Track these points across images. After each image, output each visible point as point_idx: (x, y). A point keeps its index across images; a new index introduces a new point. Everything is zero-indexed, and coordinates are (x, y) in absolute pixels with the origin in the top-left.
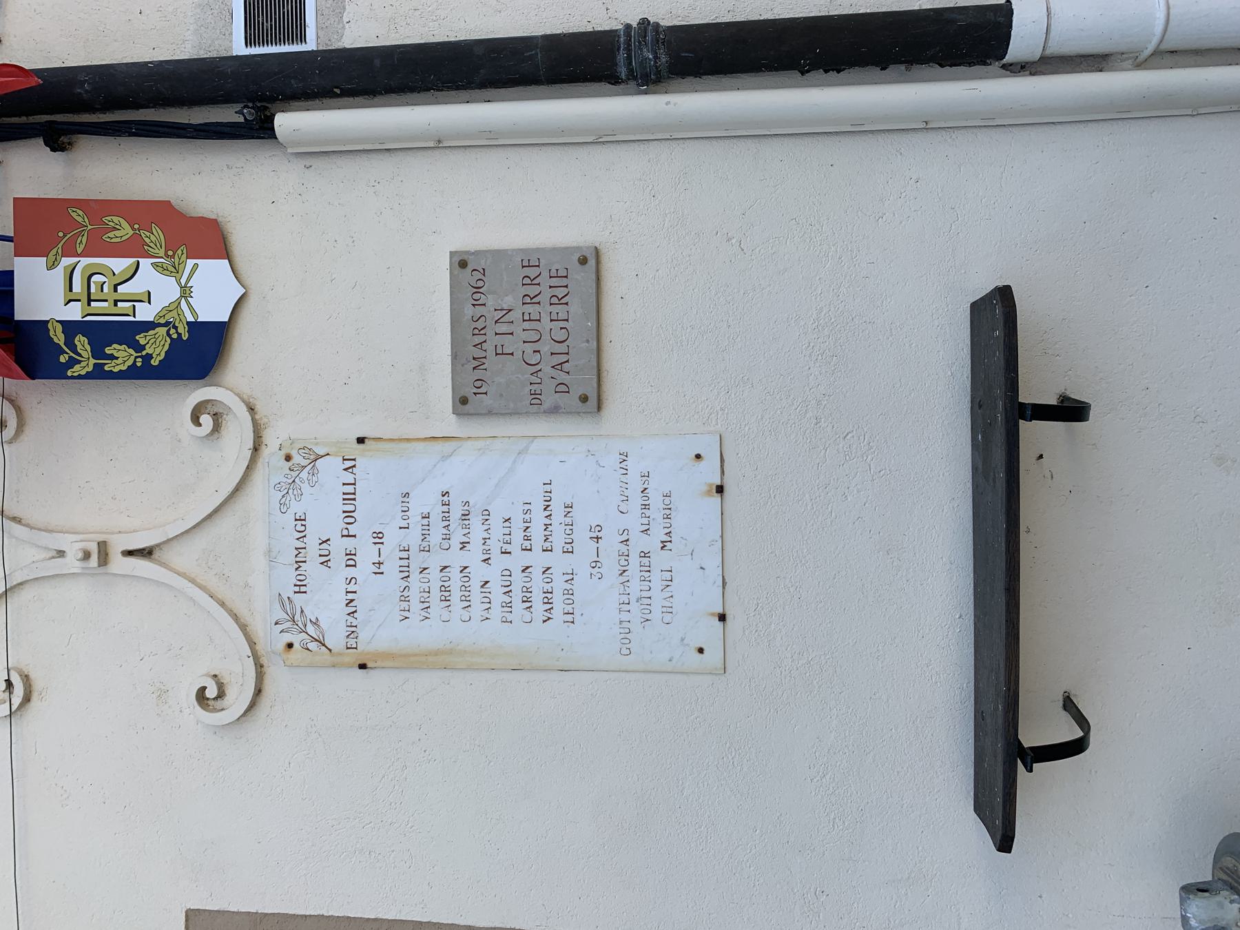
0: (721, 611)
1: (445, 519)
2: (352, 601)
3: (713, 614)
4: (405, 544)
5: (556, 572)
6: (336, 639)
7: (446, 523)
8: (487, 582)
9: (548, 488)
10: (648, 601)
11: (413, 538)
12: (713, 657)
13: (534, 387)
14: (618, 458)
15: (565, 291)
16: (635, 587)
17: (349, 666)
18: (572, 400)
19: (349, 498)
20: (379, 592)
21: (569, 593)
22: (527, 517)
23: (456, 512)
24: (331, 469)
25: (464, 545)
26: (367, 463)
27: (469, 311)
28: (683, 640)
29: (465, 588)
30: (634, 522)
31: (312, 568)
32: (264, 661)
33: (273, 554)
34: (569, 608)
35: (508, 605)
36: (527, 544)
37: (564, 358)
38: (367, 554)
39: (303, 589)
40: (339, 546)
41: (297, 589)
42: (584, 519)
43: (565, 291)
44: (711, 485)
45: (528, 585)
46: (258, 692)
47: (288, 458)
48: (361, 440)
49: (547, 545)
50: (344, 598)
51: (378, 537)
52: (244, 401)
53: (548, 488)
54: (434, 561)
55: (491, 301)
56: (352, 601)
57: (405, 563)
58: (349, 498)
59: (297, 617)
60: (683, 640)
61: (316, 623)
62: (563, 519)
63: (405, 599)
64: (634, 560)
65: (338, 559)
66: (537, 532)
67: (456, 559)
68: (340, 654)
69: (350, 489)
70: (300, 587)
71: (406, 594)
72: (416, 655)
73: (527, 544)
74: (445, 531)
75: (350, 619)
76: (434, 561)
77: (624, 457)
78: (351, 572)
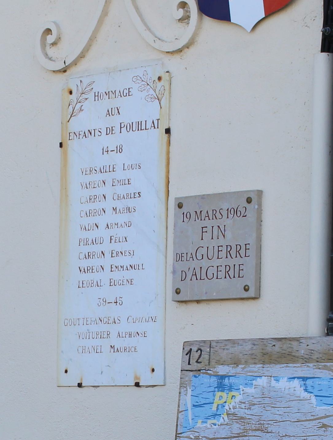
0: (83, 385)
3: (81, 379)
6: (76, 125)
10: (88, 337)
15: (232, 276)
22: (127, 253)
23: (131, 203)
27: (225, 206)
30: (124, 327)
37: (198, 277)
38: (111, 142)
43: (232, 276)
44: (139, 379)
50: (91, 128)
55: (229, 222)
77: (154, 320)
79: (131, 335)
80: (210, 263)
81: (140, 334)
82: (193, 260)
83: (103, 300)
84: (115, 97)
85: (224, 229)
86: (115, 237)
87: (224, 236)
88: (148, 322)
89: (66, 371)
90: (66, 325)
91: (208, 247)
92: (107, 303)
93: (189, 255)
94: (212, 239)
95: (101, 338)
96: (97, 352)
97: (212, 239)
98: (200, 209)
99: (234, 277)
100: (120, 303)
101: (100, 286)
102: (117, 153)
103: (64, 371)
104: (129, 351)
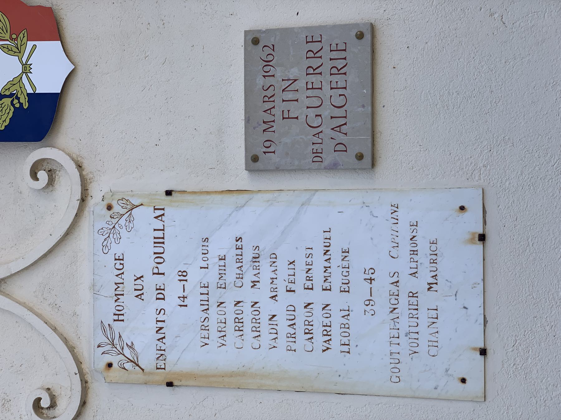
0: (482, 346)
1: (239, 261)
2: (161, 328)
3: (475, 349)
4: (205, 282)
5: (334, 309)
6: (148, 360)
7: (240, 264)
8: (274, 316)
9: (327, 235)
10: (416, 336)
11: (212, 277)
12: (474, 386)
14: (390, 209)
15: (343, 62)
16: (404, 323)
17: (158, 384)
18: (349, 158)
19: (159, 241)
20: (183, 321)
21: (346, 327)
22: (309, 260)
23: (248, 255)
24: (144, 217)
25: (254, 284)
26: (175, 213)
27: (260, 81)
28: (447, 371)
29: (256, 320)
30: (403, 265)
31: (129, 299)
32: (88, 378)
33: (97, 288)
34: (345, 340)
35: (293, 336)
36: (309, 284)
37: (343, 121)
39: (121, 318)
41: (116, 317)
42: (359, 263)
43: (343, 62)
44: (473, 234)
45: (310, 319)
46: (83, 403)
47: (109, 208)
48: (169, 193)
49: (327, 285)
50: (154, 326)
51: (183, 274)
52: (73, 159)
53: (327, 235)
54: (230, 297)
55: (279, 73)
56: (161, 328)
57: (205, 297)
58: (159, 241)
59: (116, 341)
60: (447, 371)
61: (131, 347)
62: (340, 263)
63: (205, 328)
64: (404, 299)
65: (150, 293)
66: (318, 274)
67: (248, 295)
68: (150, 373)
69: (160, 234)
70: (119, 316)
71: (206, 324)
72: (214, 376)
73: (309, 284)
74: (239, 271)
75: (160, 344)
76: (230, 297)
77: (395, 208)
78: (161, 304)
79: (414, 251)
80: (327, 103)
81: (414, 234)
82: (321, 132)
83: (367, 305)
85: (286, 81)
86: (288, 284)
87: (295, 80)
88: (397, 219)
89: (463, 381)
91: (308, 107)
92: (371, 298)
93: (316, 140)
94: (297, 100)
95: (417, 309)
96: (437, 318)
97: (297, 100)
98: (260, 125)
99: (345, 59)
100: (372, 273)
101: (349, 310)
102: (186, 280)
103: (463, 385)
104: (436, 255)
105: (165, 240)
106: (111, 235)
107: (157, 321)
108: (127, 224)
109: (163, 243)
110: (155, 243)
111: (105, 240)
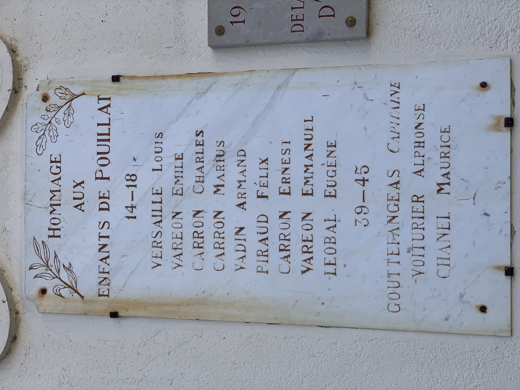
0: (508, 263)
1: (199, 160)
2: (104, 246)
3: (498, 268)
4: (157, 187)
5: (317, 219)
7: (200, 165)
8: (242, 229)
9: (309, 125)
10: (421, 252)
11: (166, 180)
12: (497, 317)
13: (296, 12)
14: (389, 90)
16: (406, 236)
17: (101, 315)
18: (337, 26)
19: (104, 139)
20: (131, 237)
21: (331, 241)
22: (286, 157)
23: (210, 153)
24: (86, 108)
25: (218, 188)
26: (122, 103)
28: (461, 296)
29: (219, 235)
30: (406, 162)
31: (66, 211)
32: (20, 307)
33: (29, 197)
34: (331, 259)
35: (264, 254)
36: (285, 187)
38: (120, 199)
39: (57, 233)
40: (92, 189)
41: (51, 233)
42: (348, 160)
44: (498, 118)
45: (286, 232)
46: (13, 339)
47: (45, 98)
48: (116, 79)
49: (308, 188)
51: (132, 178)
52: (5, 42)
53: (309, 125)
54: (188, 206)
56: (104, 246)
57: (157, 206)
58: (104, 139)
59: (51, 262)
60: (461, 296)
61: (69, 269)
62: (325, 160)
63: (157, 245)
64: (406, 205)
65: (92, 202)
66: (297, 174)
67: (210, 203)
68: (91, 301)
69: (104, 129)
70: (54, 232)
71: (158, 239)
72: (167, 304)
73: (285, 187)
74: (199, 173)
75: (103, 265)
76: (188, 206)
78: (105, 216)
81: (420, 121)
83: (359, 213)
84: (60, 191)
88: (398, 103)
89: (483, 309)
90: (398, 285)
92: (363, 204)
95: (423, 218)
96: (449, 228)
100: (365, 173)
101: (335, 220)
102: (135, 186)
104: (449, 146)
105: (111, 137)
106: (47, 133)
107: (100, 237)
108: (66, 118)
109: (108, 140)
110: (98, 140)
111: (40, 138)
